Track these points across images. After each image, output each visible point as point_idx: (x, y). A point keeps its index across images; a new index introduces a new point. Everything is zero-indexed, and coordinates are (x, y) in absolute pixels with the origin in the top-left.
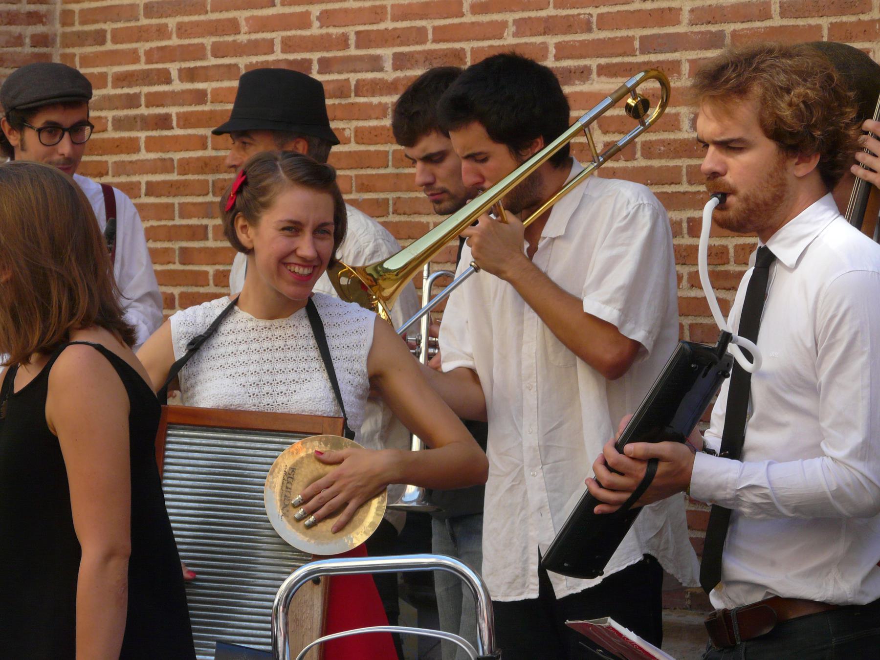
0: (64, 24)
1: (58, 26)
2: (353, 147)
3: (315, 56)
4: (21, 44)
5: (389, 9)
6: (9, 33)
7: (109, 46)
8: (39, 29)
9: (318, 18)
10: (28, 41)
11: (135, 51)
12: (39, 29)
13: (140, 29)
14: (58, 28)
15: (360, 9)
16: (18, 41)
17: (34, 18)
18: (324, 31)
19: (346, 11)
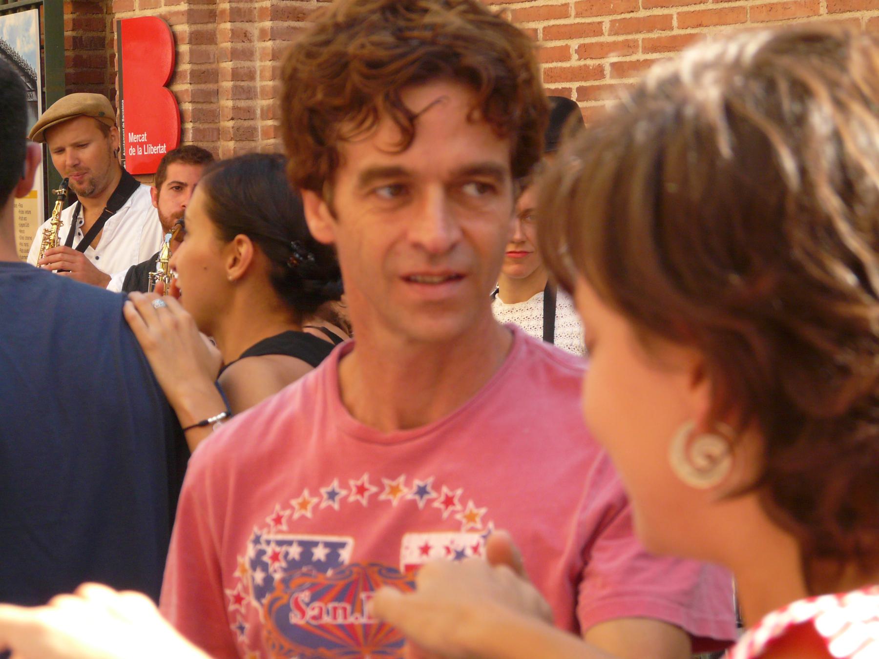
3: (574, 85)
5: (640, 42)
9: (576, 51)
18: (582, 63)
19: (601, 45)
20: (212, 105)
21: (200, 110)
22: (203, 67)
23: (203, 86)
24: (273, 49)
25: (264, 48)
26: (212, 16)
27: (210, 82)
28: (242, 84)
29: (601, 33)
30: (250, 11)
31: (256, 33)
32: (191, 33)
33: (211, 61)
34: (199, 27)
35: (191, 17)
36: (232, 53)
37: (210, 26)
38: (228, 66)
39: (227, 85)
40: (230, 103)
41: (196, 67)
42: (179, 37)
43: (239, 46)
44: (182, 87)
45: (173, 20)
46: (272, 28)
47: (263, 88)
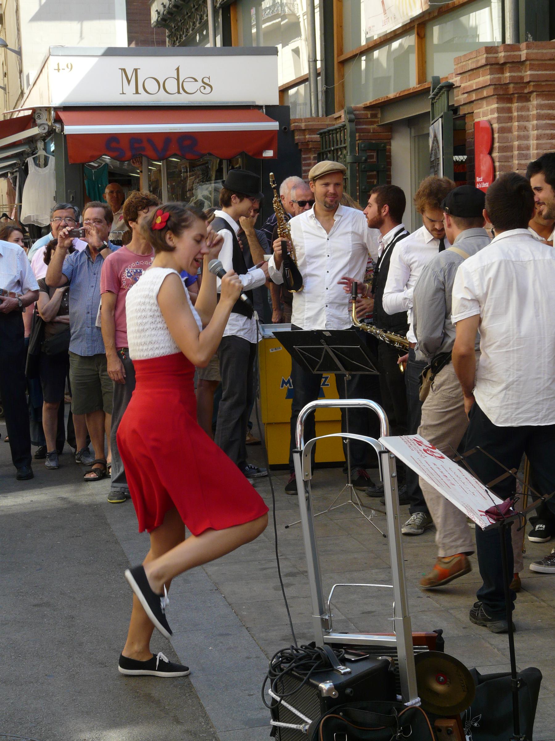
6: (552, 143)
21: (503, 166)
22: (505, 145)
23: (505, 154)
25: (534, 134)
26: (510, 119)
28: (523, 152)
30: (528, 116)
31: (531, 127)
32: (499, 128)
34: (503, 125)
35: (499, 120)
36: (518, 137)
37: (509, 124)
38: (516, 143)
39: (516, 153)
40: (516, 162)
41: (501, 145)
42: (494, 130)
43: (522, 133)
44: (495, 154)
45: (492, 123)
46: (537, 124)
47: (533, 153)
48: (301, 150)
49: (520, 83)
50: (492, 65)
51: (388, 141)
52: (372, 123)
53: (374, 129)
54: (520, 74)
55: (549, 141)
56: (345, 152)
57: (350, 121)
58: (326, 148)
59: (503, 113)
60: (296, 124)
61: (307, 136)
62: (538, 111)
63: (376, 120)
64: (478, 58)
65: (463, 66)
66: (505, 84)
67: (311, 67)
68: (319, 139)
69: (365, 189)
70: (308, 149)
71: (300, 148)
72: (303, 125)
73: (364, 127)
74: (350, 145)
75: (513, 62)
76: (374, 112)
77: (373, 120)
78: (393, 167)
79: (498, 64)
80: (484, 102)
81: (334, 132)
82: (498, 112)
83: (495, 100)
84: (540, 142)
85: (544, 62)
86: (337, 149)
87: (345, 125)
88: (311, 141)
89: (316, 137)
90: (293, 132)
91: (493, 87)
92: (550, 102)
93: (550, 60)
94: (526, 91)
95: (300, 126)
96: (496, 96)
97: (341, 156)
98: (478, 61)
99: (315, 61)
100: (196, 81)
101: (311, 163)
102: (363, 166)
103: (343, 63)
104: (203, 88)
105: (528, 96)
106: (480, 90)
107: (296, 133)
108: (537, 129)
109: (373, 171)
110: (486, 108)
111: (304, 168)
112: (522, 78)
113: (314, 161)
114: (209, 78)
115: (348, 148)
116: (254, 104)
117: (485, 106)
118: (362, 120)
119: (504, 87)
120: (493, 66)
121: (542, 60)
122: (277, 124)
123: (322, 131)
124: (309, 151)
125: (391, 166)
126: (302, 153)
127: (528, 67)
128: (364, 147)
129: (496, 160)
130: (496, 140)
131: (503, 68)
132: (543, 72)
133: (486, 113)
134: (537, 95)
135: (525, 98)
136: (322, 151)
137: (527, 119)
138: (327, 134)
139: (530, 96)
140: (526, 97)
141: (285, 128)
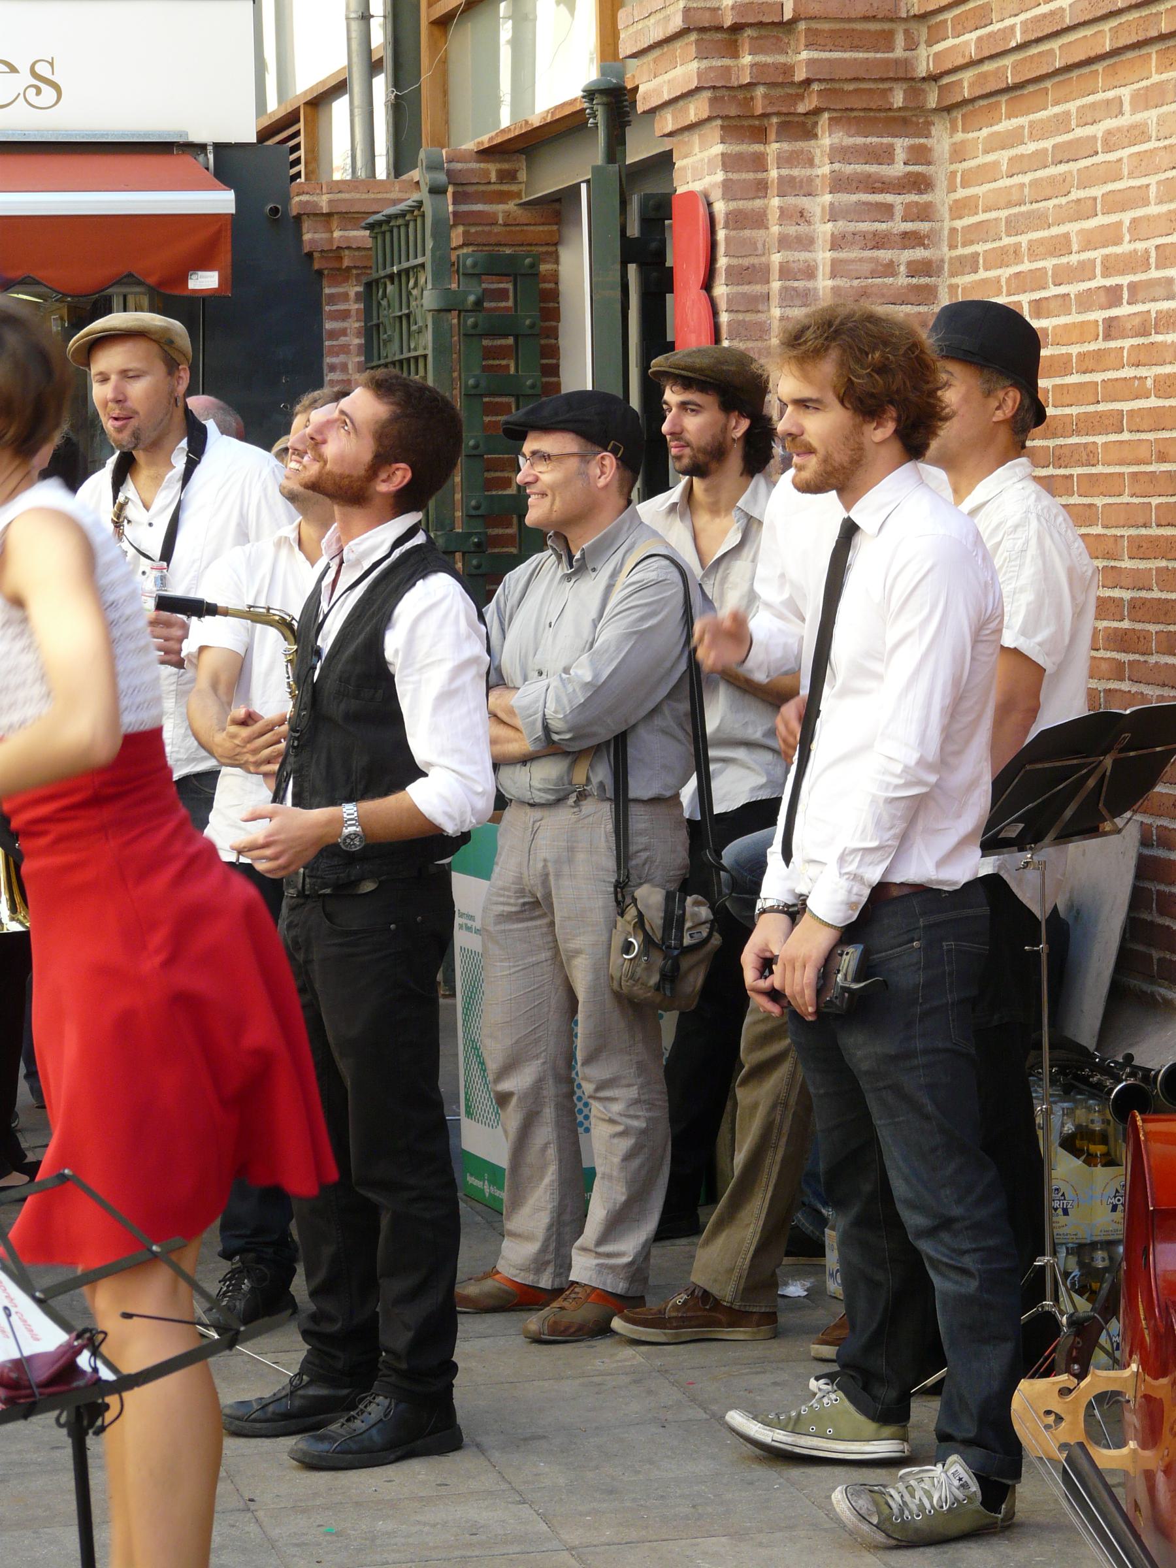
0: (952, 247)
1: (946, 249)
2: (1153, 402)
4: (894, 274)
6: (876, 260)
7: (982, 274)
8: (919, 253)
10: (902, 269)
11: (998, 280)
12: (919, 253)
13: (1003, 250)
14: (946, 253)
15: (1159, 216)
16: (889, 269)
17: (911, 239)
19: (1148, 218)
20: (760, 315)
21: (739, 322)
22: (746, 262)
23: (746, 289)
24: (833, 234)
25: (825, 233)
26: (761, 188)
27: (757, 283)
28: (796, 284)
29: (1146, 203)
30: (810, 180)
32: (728, 214)
33: (760, 252)
34: (741, 204)
36: (780, 241)
37: (758, 203)
38: (776, 258)
39: (776, 285)
40: (776, 312)
41: (735, 262)
43: (792, 230)
44: (721, 290)
45: (712, 199)
46: (832, 204)
48: (320, 273)
49: (782, 82)
50: (702, 30)
51: (553, 249)
52: (502, 197)
53: (507, 214)
54: (781, 59)
55: (868, 254)
56: (422, 281)
57: (437, 191)
58: (385, 268)
59: (739, 171)
60: (304, 198)
61: (337, 234)
62: (837, 166)
63: (514, 188)
64: (669, 11)
65: (637, 32)
66: (741, 87)
67: (354, 35)
68: (369, 243)
69: (476, 386)
70: (339, 269)
71: (316, 266)
72: (323, 202)
73: (479, 207)
74: (433, 261)
75: (761, 24)
76: (506, 166)
77: (505, 188)
78: (563, 327)
79: (719, 28)
80: (695, 138)
81: (400, 221)
82: (726, 167)
83: (717, 134)
84: (842, 255)
85: (847, 26)
86: (407, 271)
87: (420, 204)
88: (348, 248)
89: (361, 236)
90: (298, 218)
91: (707, 94)
92: (869, 140)
93: (866, 19)
94: (801, 108)
95: (315, 204)
96: (719, 122)
97: (415, 292)
98: (667, 18)
99: (366, 17)
100: (13, 69)
101: (349, 311)
102: (471, 321)
103: (443, 23)
104: (33, 90)
105: (809, 121)
106: (681, 103)
107: (306, 225)
108: (833, 219)
109: (506, 336)
110: (700, 156)
111: (328, 325)
112: (788, 69)
113: (356, 306)
114: (52, 64)
115: (428, 267)
116: (181, 140)
117: (697, 149)
118: (470, 189)
119: (741, 96)
120: (707, 36)
121: (842, 20)
122: (230, 195)
123: (371, 219)
124: (342, 275)
125: (558, 320)
126: (325, 282)
127: (803, 41)
128: (475, 265)
129: (722, 305)
130: (721, 249)
131: (736, 41)
132: (847, 55)
133: (700, 170)
134: (829, 119)
135: (800, 127)
136: (375, 276)
137: (807, 188)
138: (385, 228)
139: (816, 123)
140: (804, 124)
141: (275, 211)
